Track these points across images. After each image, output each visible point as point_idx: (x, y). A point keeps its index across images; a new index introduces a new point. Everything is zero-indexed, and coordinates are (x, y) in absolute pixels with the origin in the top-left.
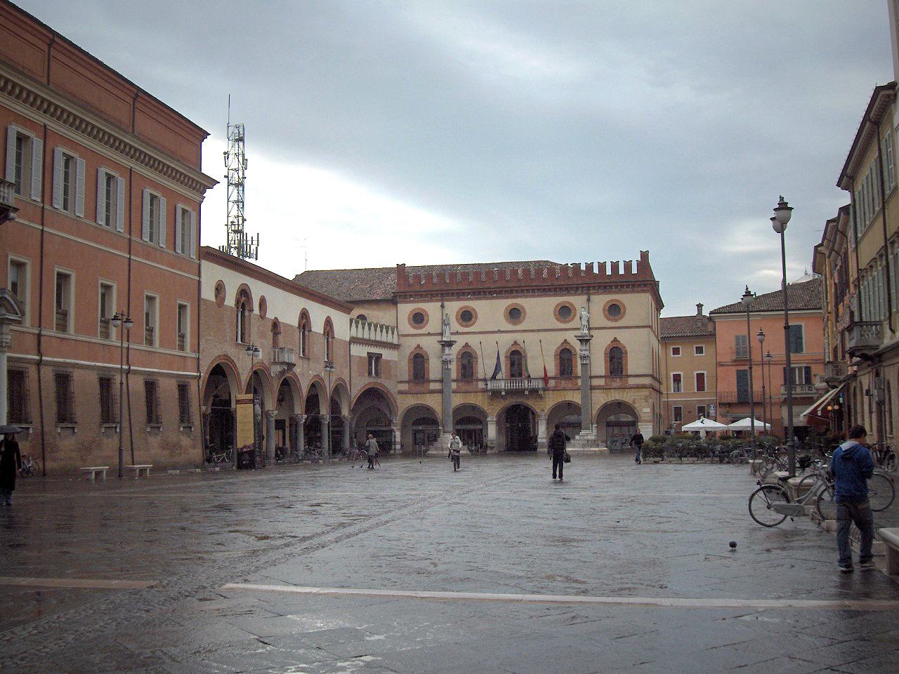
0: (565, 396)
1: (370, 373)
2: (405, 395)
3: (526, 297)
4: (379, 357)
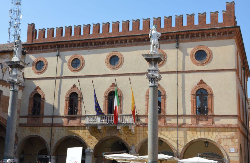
2: (24, 128)
3: (125, 46)
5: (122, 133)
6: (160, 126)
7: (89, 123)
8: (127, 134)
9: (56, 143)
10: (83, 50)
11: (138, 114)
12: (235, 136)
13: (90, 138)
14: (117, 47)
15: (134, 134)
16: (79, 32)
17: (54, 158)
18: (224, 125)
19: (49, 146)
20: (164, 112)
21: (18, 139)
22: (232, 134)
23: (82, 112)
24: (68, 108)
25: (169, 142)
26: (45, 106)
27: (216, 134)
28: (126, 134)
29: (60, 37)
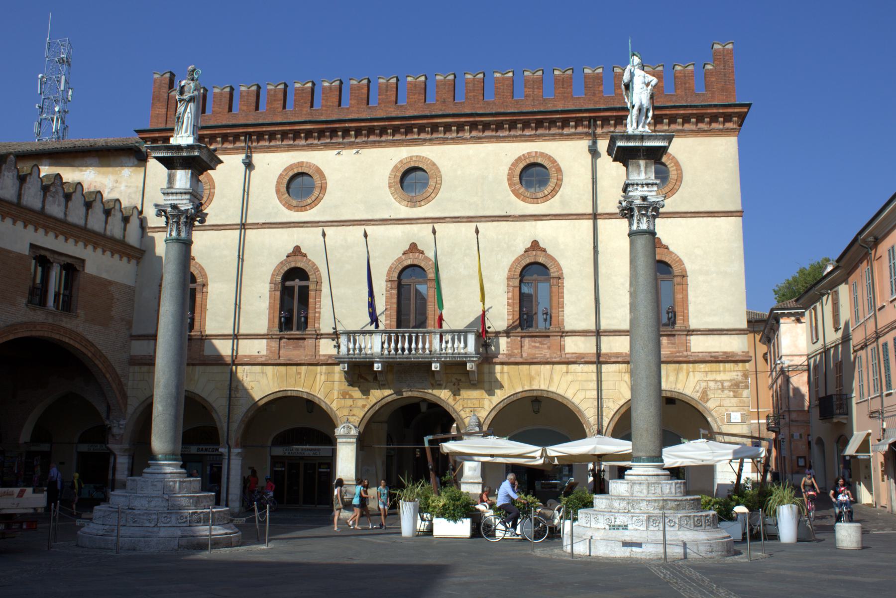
0: (531, 378)
1: (37, 296)
3: (444, 141)
4: (72, 268)
5: (442, 382)
6: (549, 360)
7: (348, 354)
8: (454, 385)
9: (245, 410)
10: (321, 150)
11: (489, 328)
12: (742, 383)
13: (347, 397)
14: (422, 145)
15: (476, 382)
16: (310, 98)
17: (239, 453)
18: (717, 354)
19: (224, 420)
20: (561, 323)
21: (129, 401)
22: (736, 377)
23: (319, 324)
24: (280, 313)
25: (573, 403)
26: (208, 307)
27: (696, 379)
28: (452, 384)
29: (254, 113)
